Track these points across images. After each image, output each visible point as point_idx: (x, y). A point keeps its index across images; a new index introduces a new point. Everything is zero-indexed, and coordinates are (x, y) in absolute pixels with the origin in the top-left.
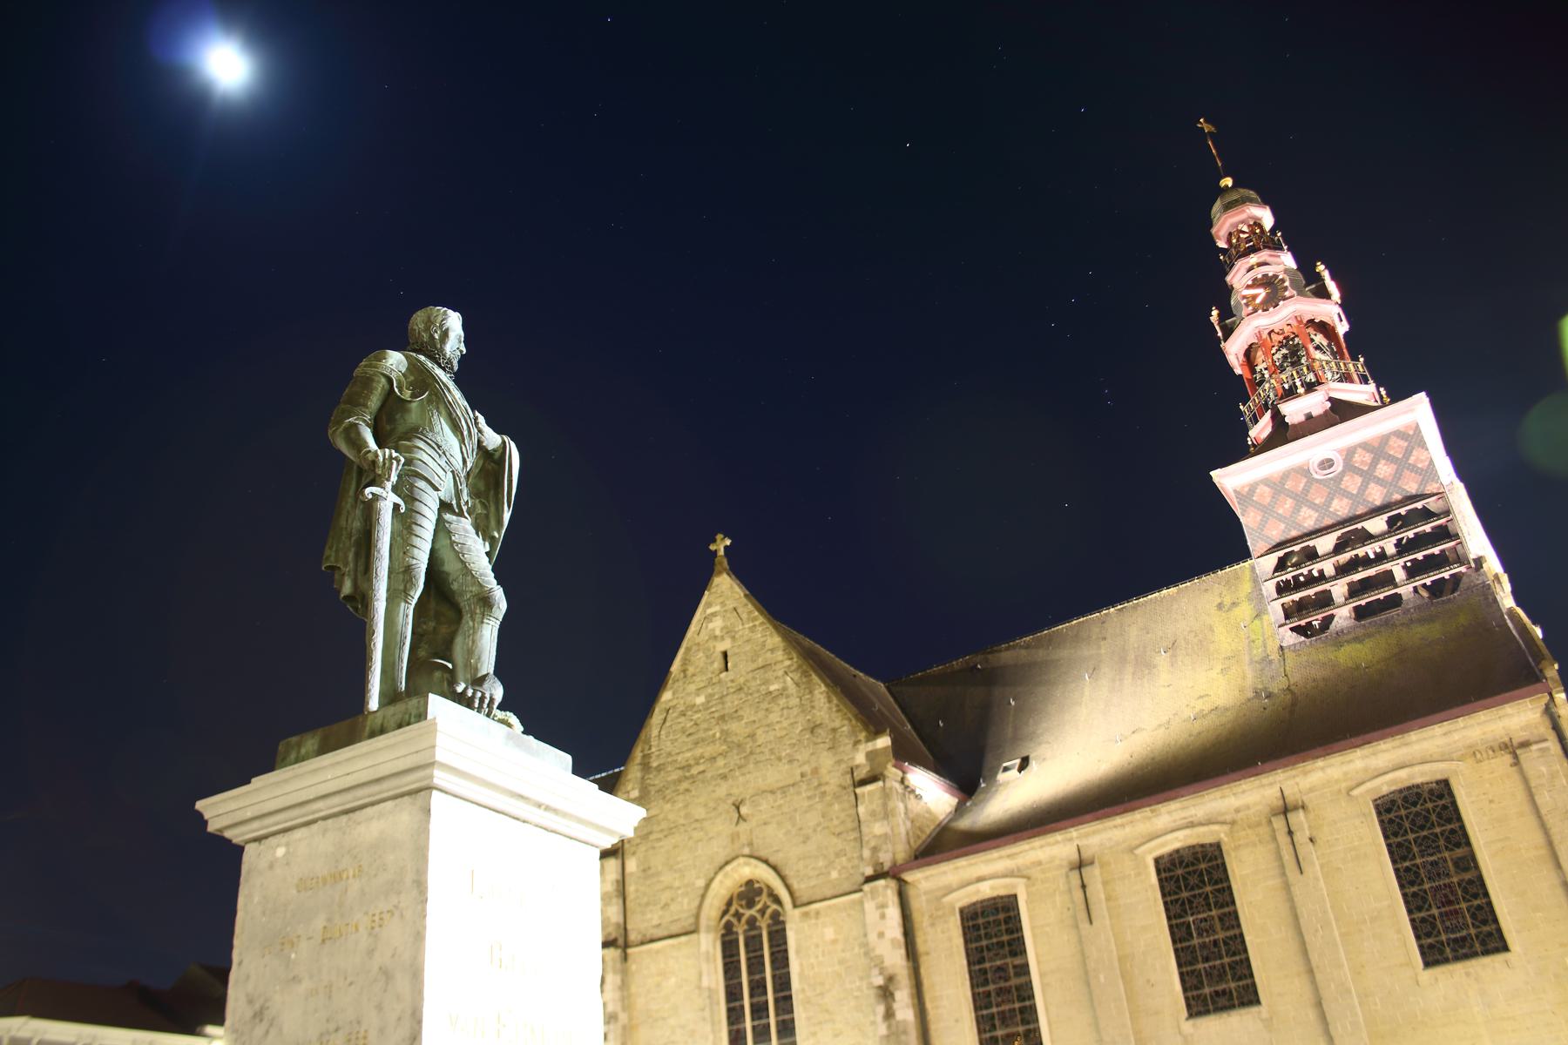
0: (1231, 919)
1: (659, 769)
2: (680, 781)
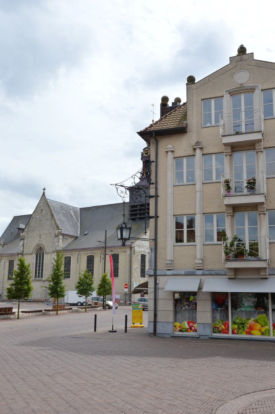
0: (93, 266)
1: (31, 227)
2: (33, 230)
